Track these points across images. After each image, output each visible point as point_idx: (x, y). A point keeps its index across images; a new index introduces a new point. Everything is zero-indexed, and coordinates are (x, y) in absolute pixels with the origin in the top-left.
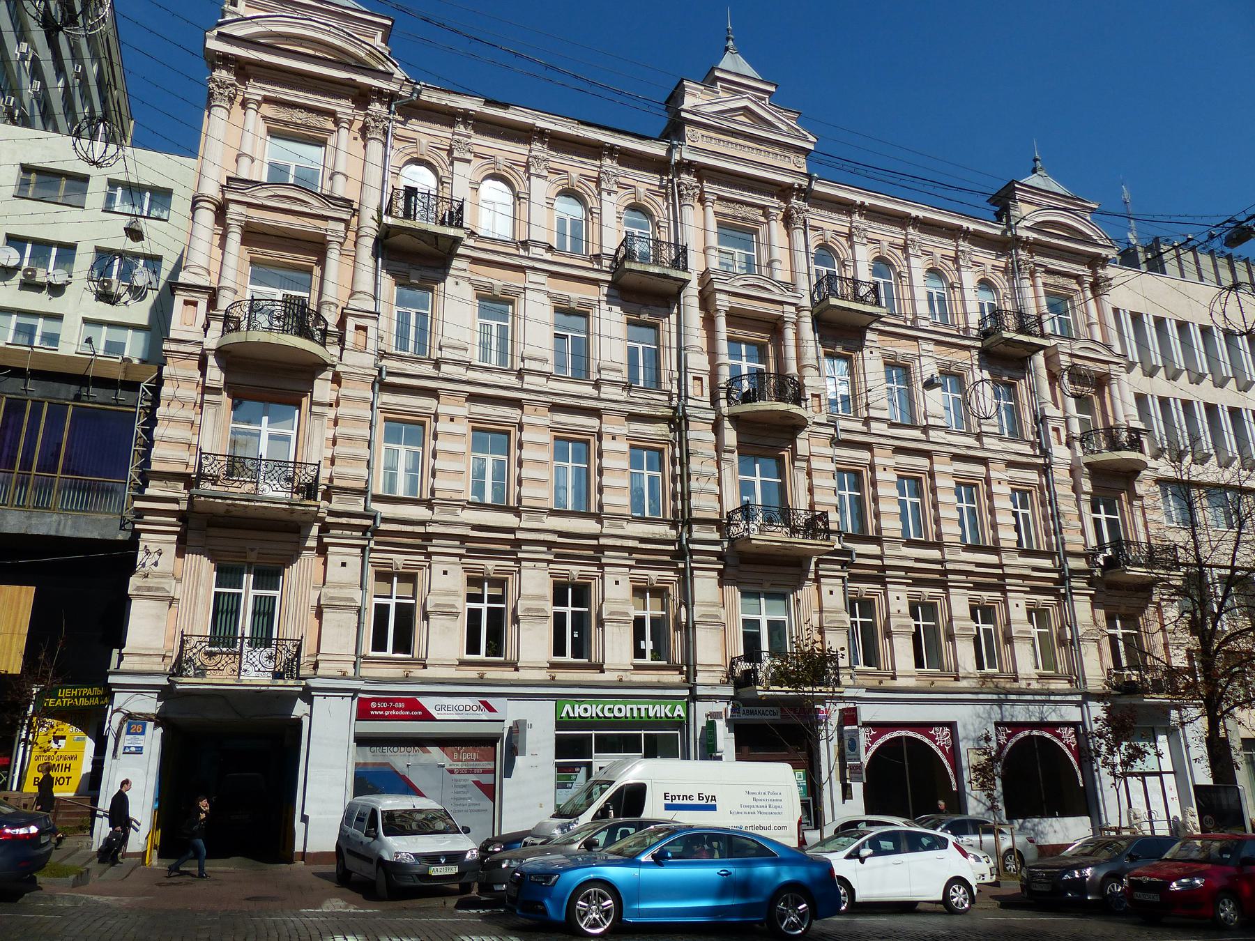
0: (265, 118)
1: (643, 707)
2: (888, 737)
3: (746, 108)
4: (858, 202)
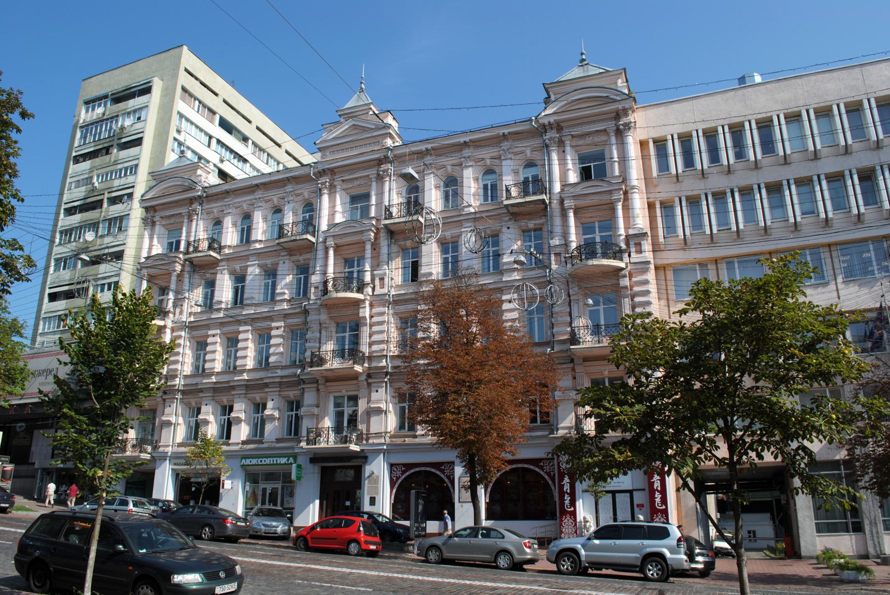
0: (164, 226)
1: (275, 459)
2: (412, 471)
3: (354, 125)
4: (424, 149)
